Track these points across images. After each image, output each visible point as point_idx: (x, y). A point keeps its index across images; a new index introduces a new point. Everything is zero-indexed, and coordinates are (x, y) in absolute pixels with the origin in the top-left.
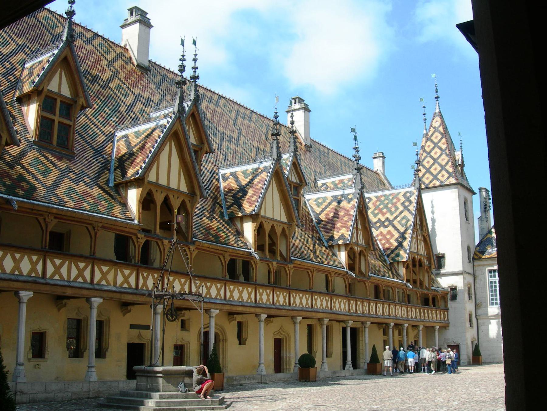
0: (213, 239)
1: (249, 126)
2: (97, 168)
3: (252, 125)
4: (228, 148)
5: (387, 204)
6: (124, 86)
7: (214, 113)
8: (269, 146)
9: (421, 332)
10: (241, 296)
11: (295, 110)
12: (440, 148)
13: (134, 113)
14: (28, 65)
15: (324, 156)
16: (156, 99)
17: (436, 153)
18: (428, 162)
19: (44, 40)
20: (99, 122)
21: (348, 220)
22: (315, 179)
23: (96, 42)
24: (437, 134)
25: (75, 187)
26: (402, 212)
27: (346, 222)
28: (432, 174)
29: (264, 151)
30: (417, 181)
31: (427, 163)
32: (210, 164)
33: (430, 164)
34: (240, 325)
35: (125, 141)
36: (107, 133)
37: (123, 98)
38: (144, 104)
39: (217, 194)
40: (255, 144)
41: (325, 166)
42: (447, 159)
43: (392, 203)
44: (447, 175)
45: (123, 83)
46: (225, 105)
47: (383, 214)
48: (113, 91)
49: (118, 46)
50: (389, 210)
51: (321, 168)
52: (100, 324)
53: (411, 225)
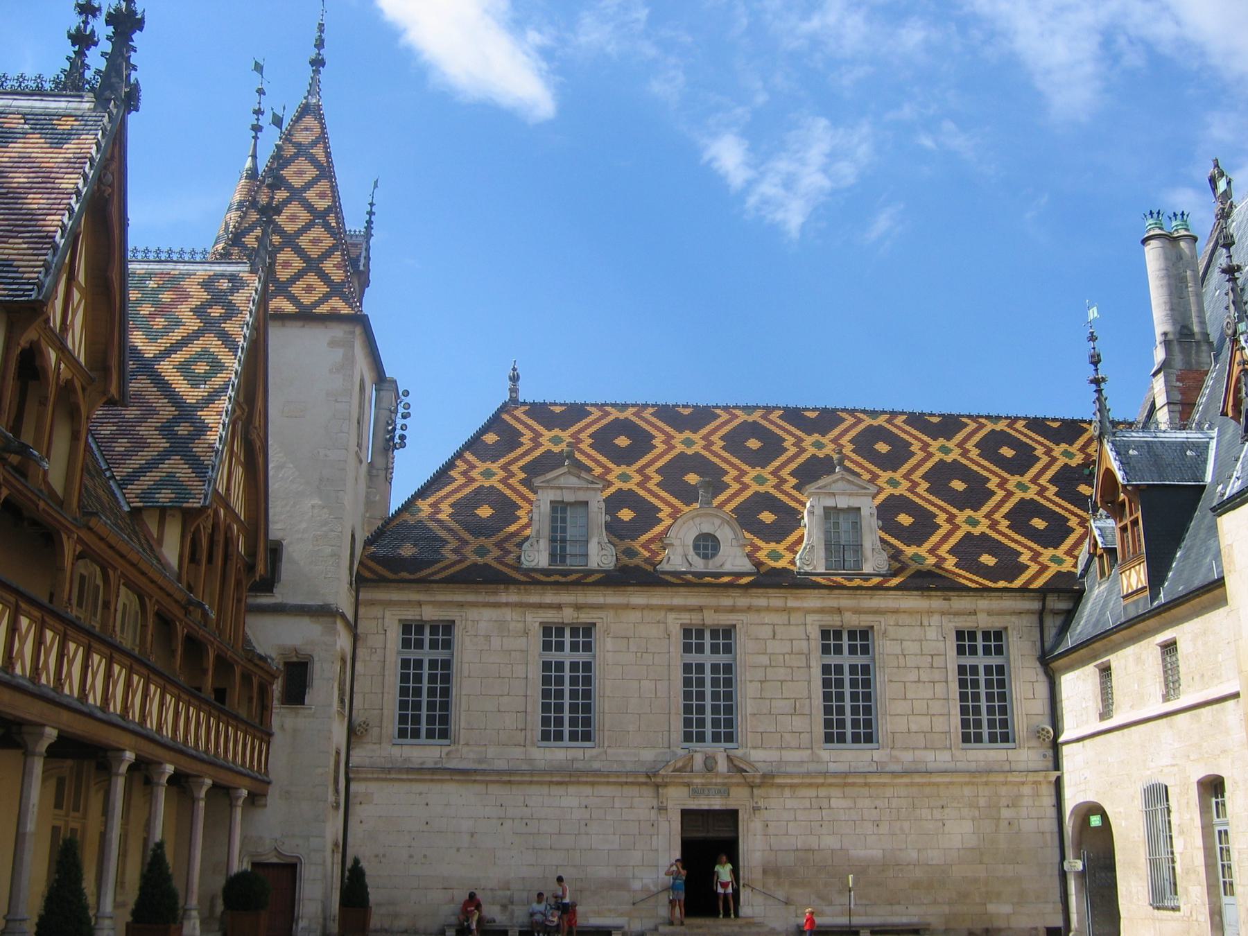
9: (202, 804)
24: (302, 163)
26: (197, 335)
42: (328, 241)
43: (157, 303)
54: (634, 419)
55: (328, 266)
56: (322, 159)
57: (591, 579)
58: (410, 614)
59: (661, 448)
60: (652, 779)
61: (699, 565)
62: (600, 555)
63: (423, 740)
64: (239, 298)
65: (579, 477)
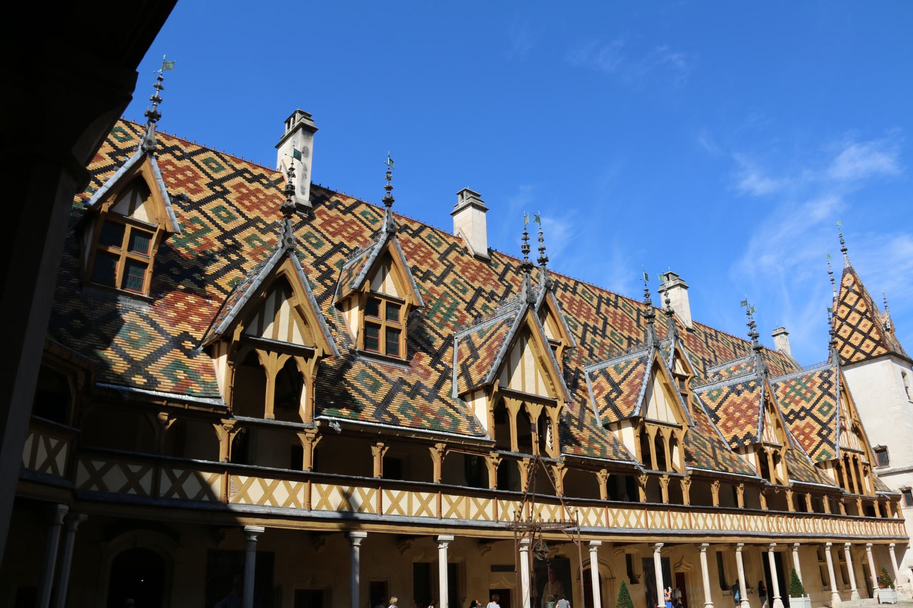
0: (586, 452)
1: (615, 314)
2: (437, 378)
3: (619, 311)
4: (593, 341)
5: (800, 389)
6: (462, 281)
7: (571, 302)
8: (642, 334)
10: (627, 522)
11: (669, 288)
12: (859, 312)
13: (476, 311)
14: (346, 267)
15: (712, 339)
16: (500, 292)
17: (854, 318)
18: (845, 331)
19: (363, 237)
20: (435, 323)
21: (754, 414)
22: (705, 369)
23: (424, 234)
24: (851, 294)
25: (411, 401)
26: (821, 397)
27: (750, 417)
28: (852, 345)
29: (638, 341)
30: (835, 358)
31: (845, 331)
32: (573, 362)
33: (848, 333)
34: (629, 558)
35: (468, 343)
36: (445, 336)
37: (460, 294)
38: (487, 299)
39: (586, 398)
40: (626, 333)
41: (714, 352)
42: (870, 324)
43: (806, 388)
44: (873, 344)
45: (460, 277)
46: (584, 292)
47: (797, 403)
48: (448, 287)
49: (449, 236)
50: (803, 397)
51: (709, 355)
52: (451, 568)
53: (835, 414)
55: (872, 334)
56: (858, 290)
64: (832, 379)
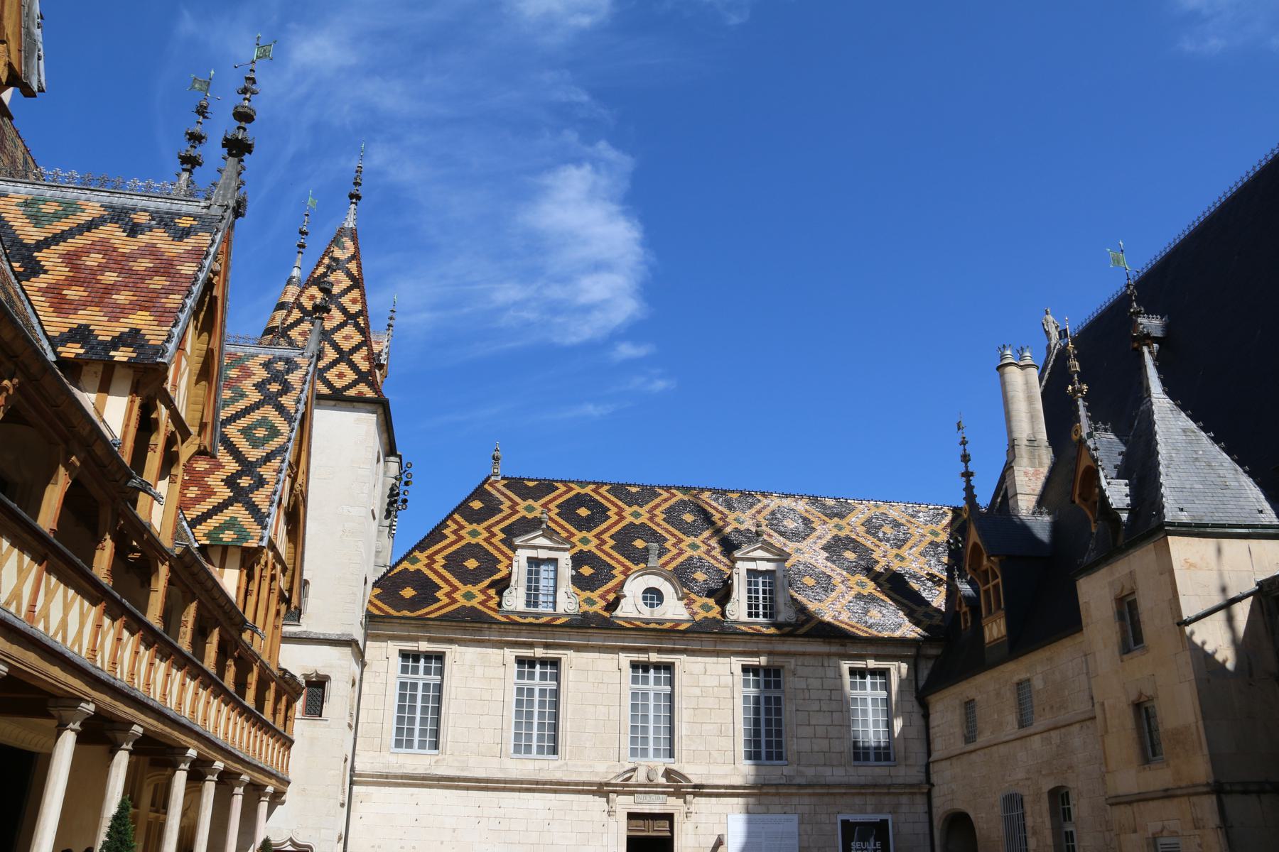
12: (344, 310)
26: (256, 406)
42: (358, 338)
44: (351, 376)
53: (282, 450)
54: (593, 494)
55: (357, 358)
57: (558, 622)
58: (409, 646)
59: (615, 518)
60: (602, 790)
61: (647, 613)
62: (568, 602)
63: (416, 749)
64: (294, 378)
65: (551, 539)
